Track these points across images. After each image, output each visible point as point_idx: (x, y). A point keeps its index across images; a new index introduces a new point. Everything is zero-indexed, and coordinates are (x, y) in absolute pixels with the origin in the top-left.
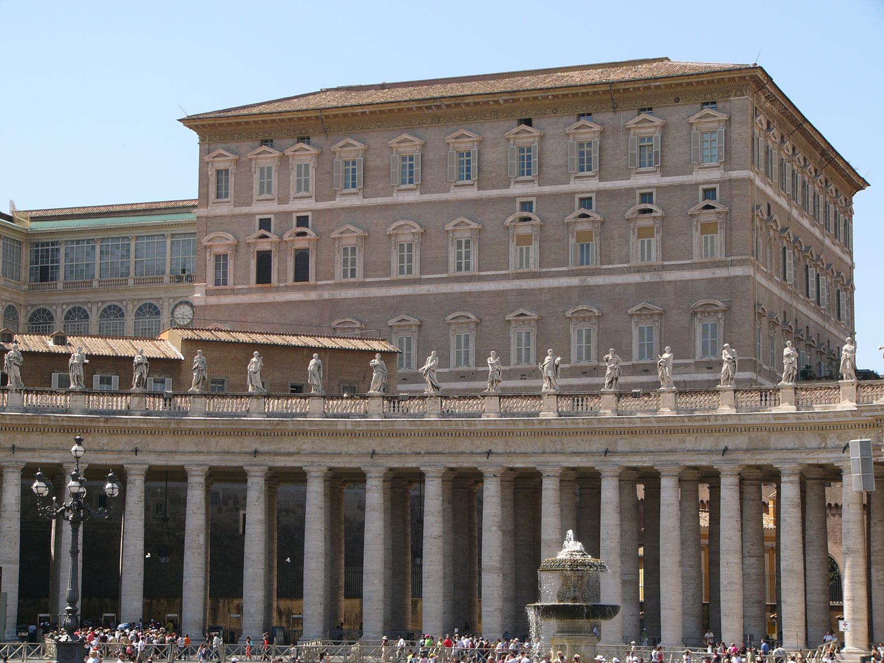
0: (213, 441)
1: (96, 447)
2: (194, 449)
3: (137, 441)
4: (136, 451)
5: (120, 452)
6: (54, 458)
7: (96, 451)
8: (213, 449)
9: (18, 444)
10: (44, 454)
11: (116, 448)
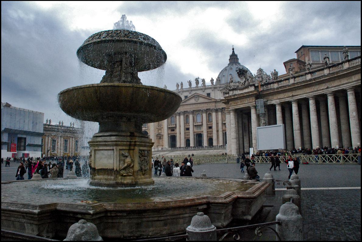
0: (353, 77)
1: (316, 90)
2: (346, 82)
3: (328, 85)
4: (328, 88)
5: (322, 90)
6: (304, 96)
7: (315, 91)
8: (354, 80)
9: (294, 94)
10: (301, 96)
11: (321, 88)
